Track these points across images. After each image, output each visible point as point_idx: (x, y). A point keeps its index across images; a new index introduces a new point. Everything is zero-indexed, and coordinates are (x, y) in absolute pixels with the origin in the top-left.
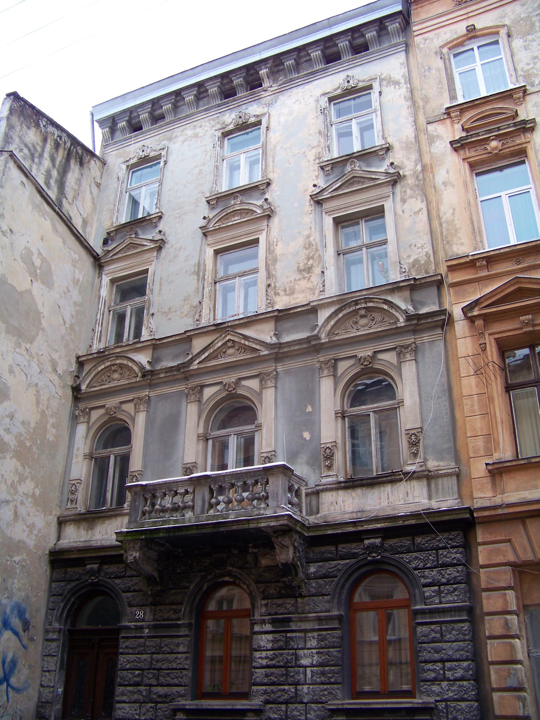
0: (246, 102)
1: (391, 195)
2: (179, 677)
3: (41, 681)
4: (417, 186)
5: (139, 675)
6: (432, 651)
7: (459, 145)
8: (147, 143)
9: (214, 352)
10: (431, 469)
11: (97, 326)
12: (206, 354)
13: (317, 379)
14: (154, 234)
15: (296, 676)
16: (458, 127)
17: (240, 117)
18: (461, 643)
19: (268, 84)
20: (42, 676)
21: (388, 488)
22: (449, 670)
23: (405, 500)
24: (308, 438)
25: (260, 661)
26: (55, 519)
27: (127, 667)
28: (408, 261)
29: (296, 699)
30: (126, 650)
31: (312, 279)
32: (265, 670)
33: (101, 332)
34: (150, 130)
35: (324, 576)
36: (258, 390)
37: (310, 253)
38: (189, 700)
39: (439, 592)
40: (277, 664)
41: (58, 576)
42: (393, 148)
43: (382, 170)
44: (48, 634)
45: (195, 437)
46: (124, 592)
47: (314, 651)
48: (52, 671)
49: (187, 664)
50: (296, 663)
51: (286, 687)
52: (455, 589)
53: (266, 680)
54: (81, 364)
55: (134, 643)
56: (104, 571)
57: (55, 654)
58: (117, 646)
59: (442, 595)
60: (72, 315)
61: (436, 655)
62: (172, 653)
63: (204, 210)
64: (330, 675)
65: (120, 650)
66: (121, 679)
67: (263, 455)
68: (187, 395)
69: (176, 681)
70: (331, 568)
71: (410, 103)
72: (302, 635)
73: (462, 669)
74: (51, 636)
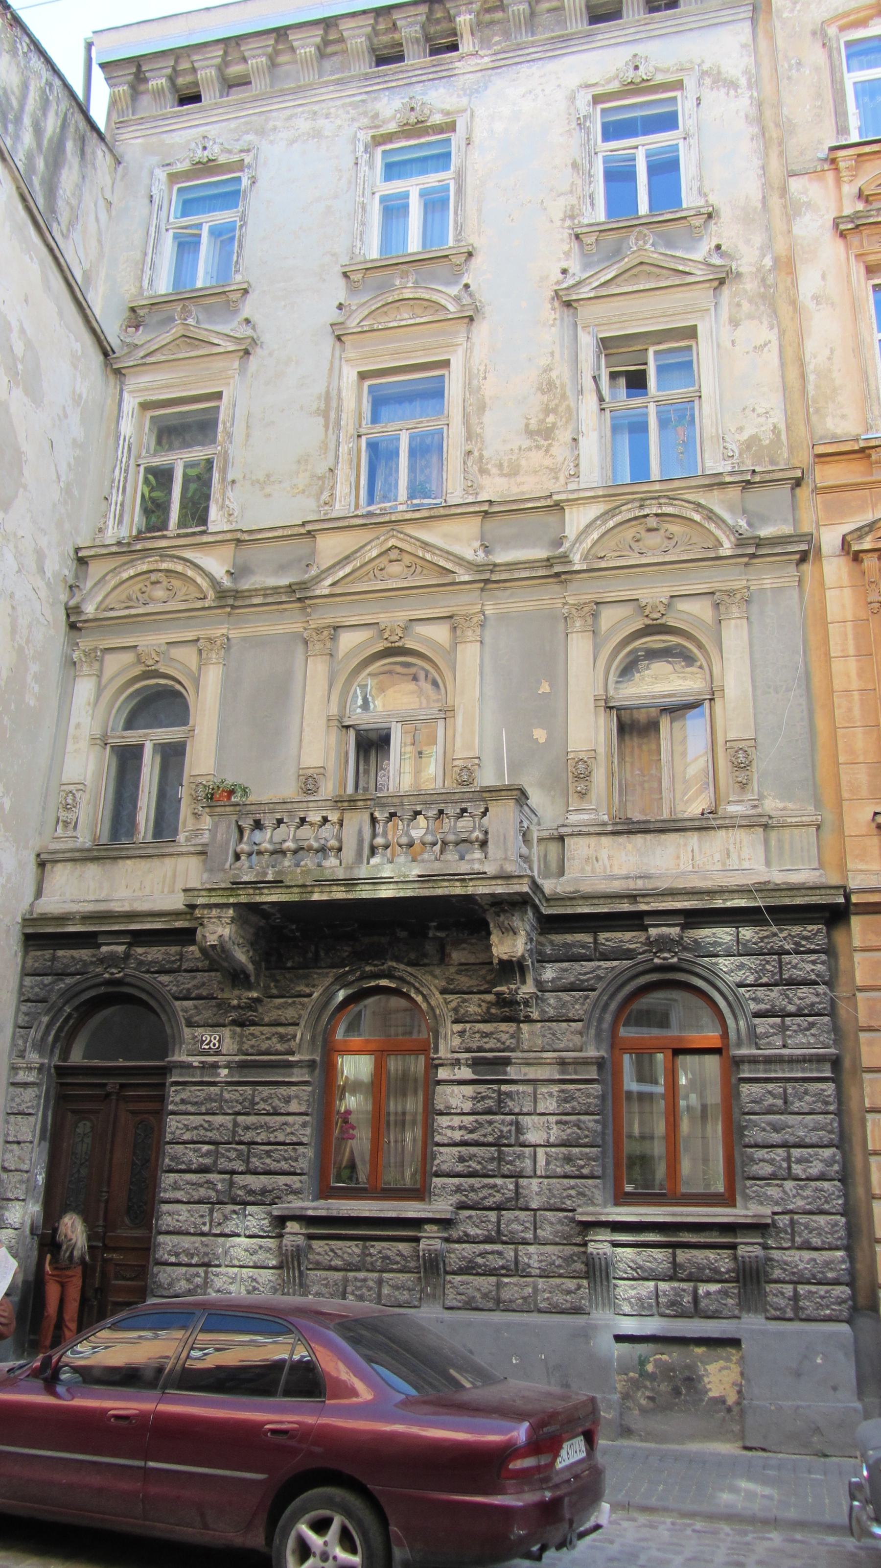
0: (424, 78)
1: (713, 308)
2: (291, 1158)
3: (3, 1161)
4: (763, 297)
5: (208, 1154)
6: (768, 1128)
7: (850, 226)
8: (212, 131)
9: (362, 566)
10: (772, 813)
11: (114, 491)
12: (348, 569)
13: (563, 636)
14: (234, 324)
15: (518, 1163)
16: (849, 189)
17: (412, 109)
18: (820, 1117)
19: (471, 49)
20: (4, 1152)
21: (693, 839)
22: (799, 1161)
23: (724, 864)
24: (542, 740)
25: (449, 1133)
26: (33, 857)
27: (187, 1137)
28: (737, 437)
29: (516, 1202)
30: (183, 1108)
31: (554, 450)
32: (459, 1149)
33: (122, 505)
34: (217, 106)
35: (570, 988)
36: (447, 646)
37: (548, 401)
38: (308, 1200)
39: (784, 1028)
40: (482, 1139)
41: (36, 965)
42: (719, 217)
43: (698, 256)
44: (17, 1074)
45: (324, 721)
46: (177, 999)
47: (553, 1119)
48: (25, 1142)
49: (306, 1135)
50: (517, 1138)
51: (499, 1181)
52: (812, 1025)
53: (460, 1168)
54: (82, 561)
55: (199, 1093)
56: (136, 959)
57: (31, 1111)
58: (162, 1099)
59: (788, 1033)
60: (69, 465)
61: (774, 1135)
62: (276, 1113)
63: (339, 291)
64: (581, 1163)
65: (171, 1107)
66: (172, 1159)
67: (456, 763)
68: (306, 642)
69: (284, 1166)
70: (586, 974)
71: (756, 130)
72: (529, 1089)
73: (821, 1161)
74: (22, 1077)
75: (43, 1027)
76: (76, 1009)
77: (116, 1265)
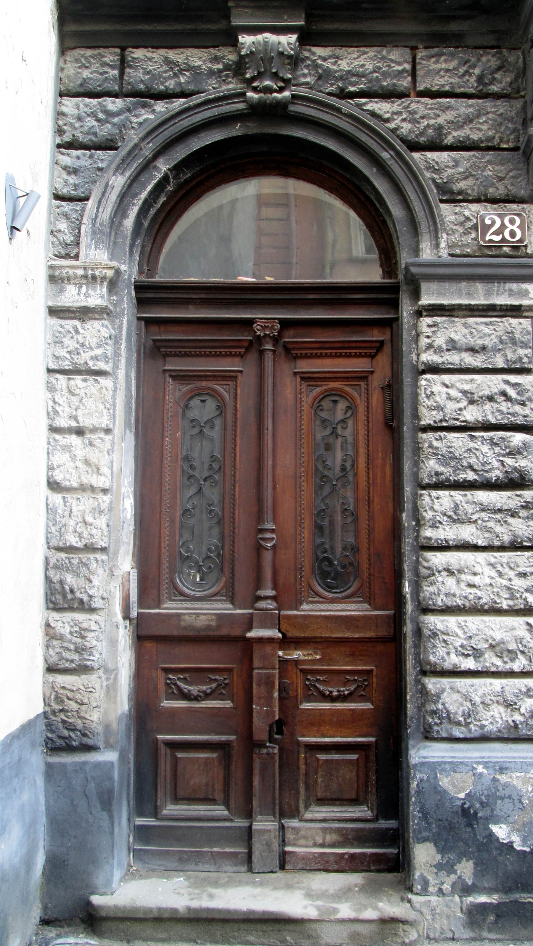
3: (50, 468)
41: (86, 73)
44: (62, 291)
46: (414, 147)
48: (94, 430)
55: (487, 330)
56: (316, 66)
57: (102, 366)
65: (427, 357)
75: (113, 196)
76: (177, 168)
77: (305, 672)
